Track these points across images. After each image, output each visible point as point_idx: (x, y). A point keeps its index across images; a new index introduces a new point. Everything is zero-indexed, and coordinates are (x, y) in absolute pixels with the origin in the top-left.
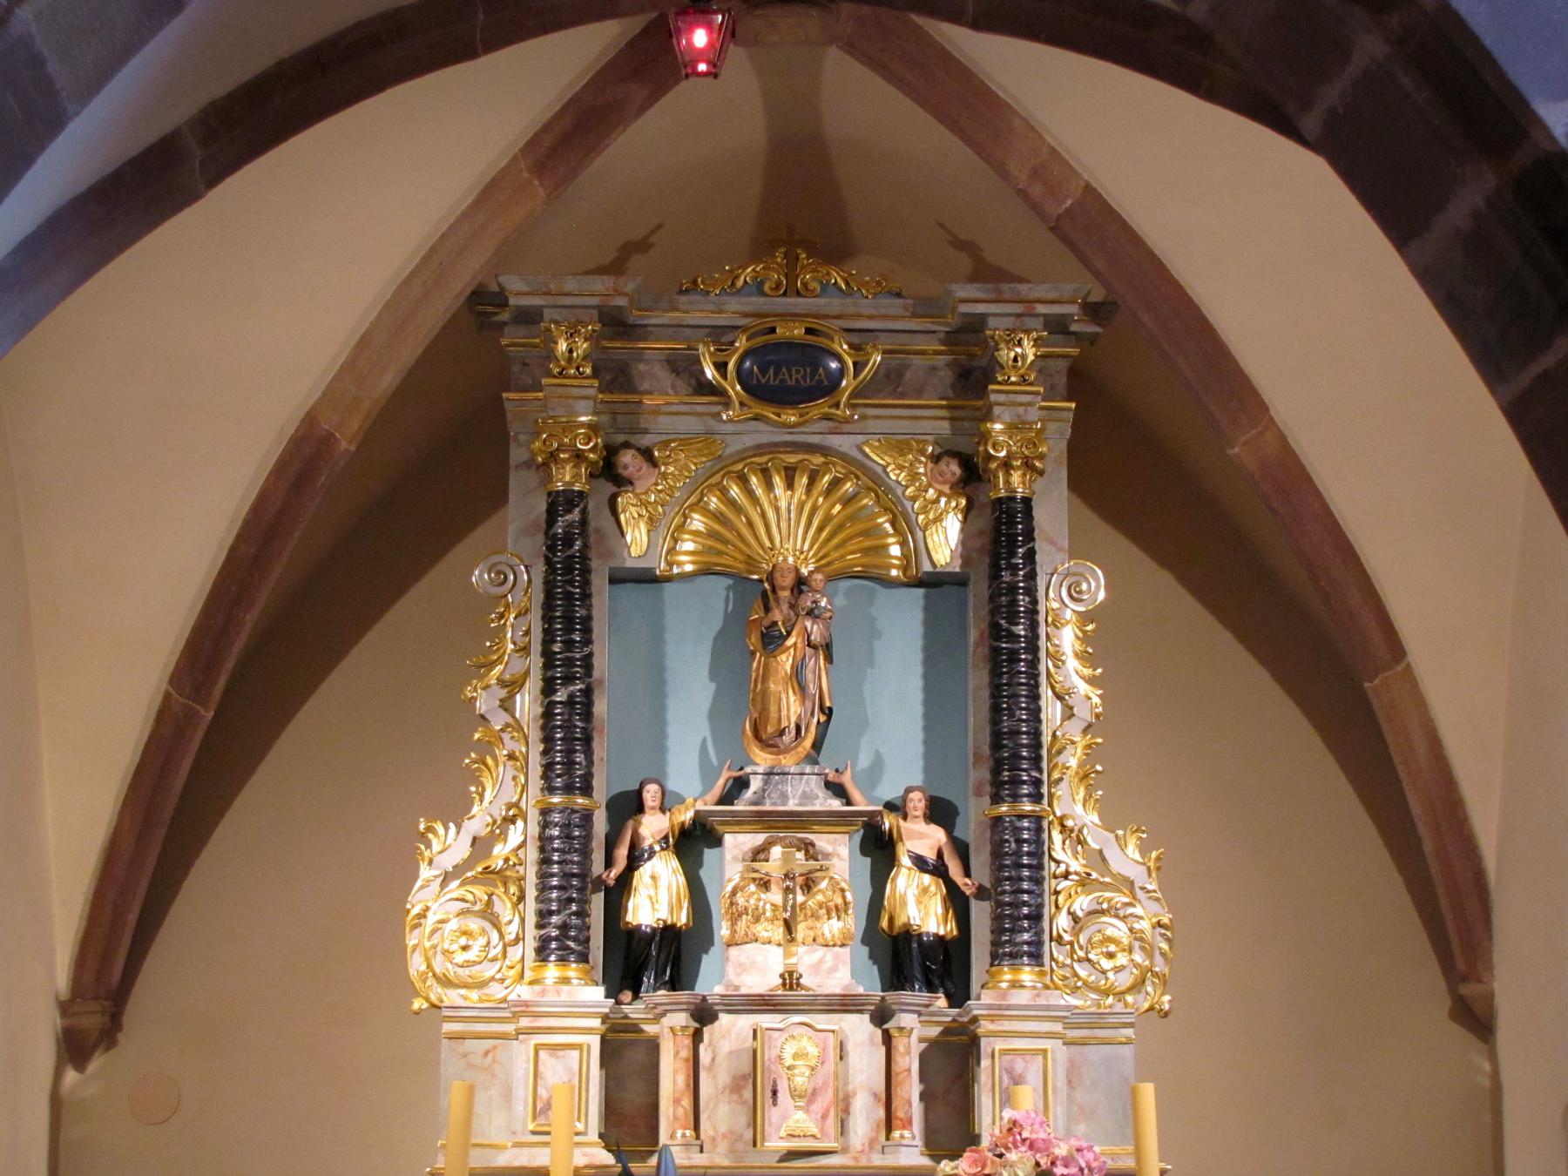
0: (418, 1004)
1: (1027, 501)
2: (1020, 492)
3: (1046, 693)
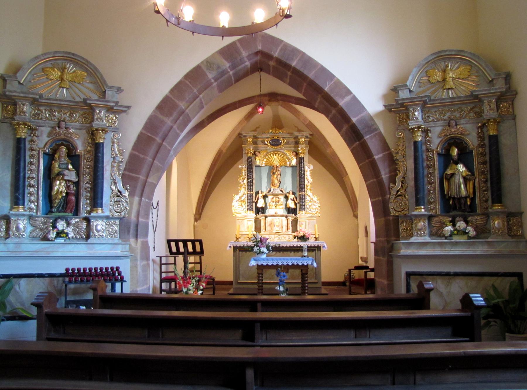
0: (234, 216)
1: (303, 157)
2: (302, 156)
3: (306, 180)
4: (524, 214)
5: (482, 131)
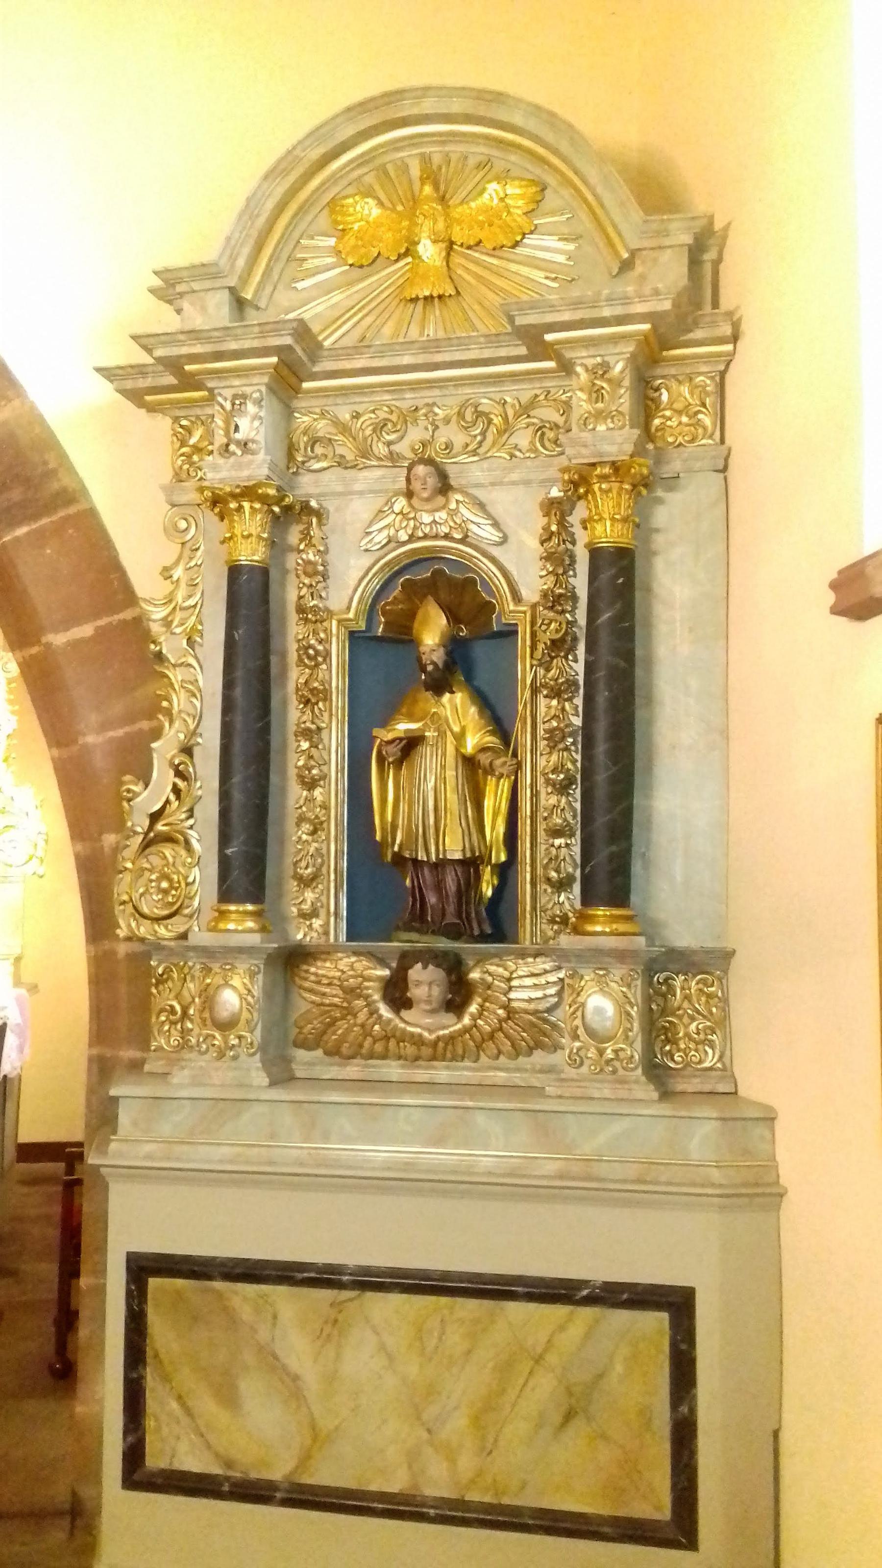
4: (735, 962)
5: (562, 523)
